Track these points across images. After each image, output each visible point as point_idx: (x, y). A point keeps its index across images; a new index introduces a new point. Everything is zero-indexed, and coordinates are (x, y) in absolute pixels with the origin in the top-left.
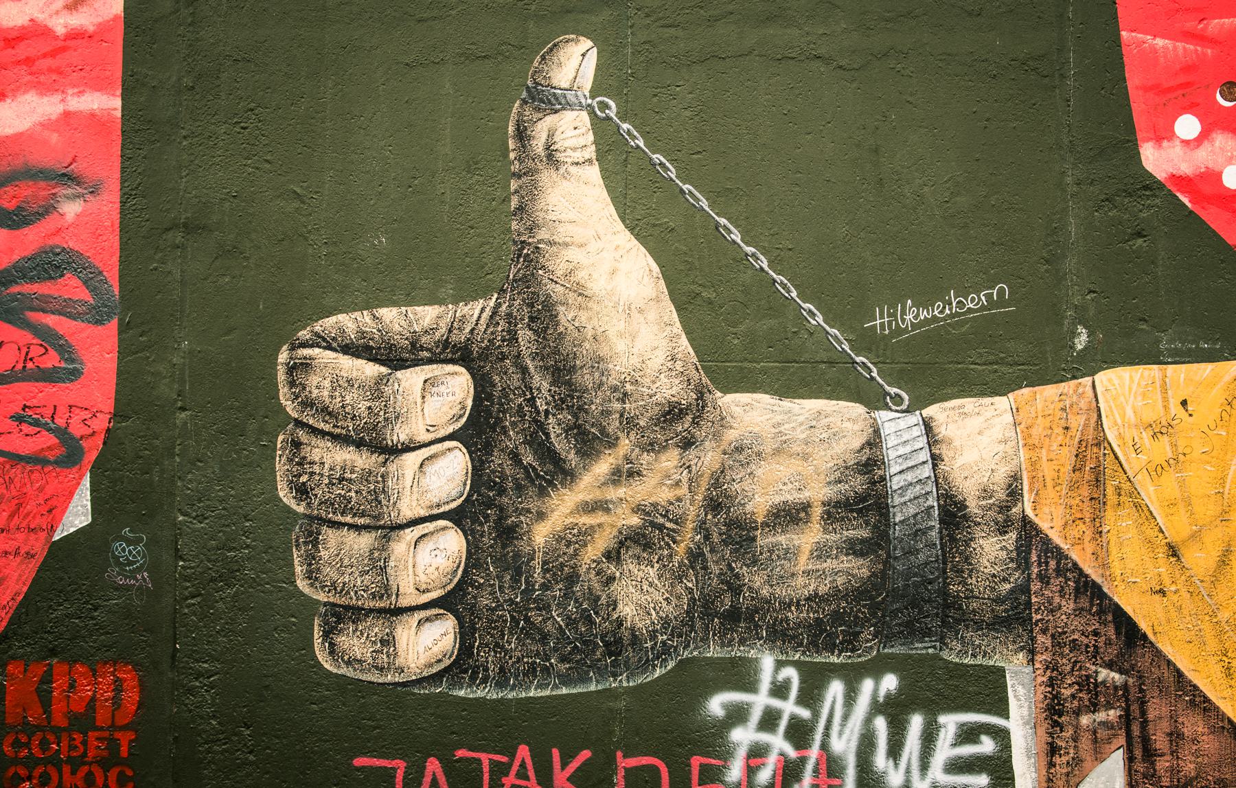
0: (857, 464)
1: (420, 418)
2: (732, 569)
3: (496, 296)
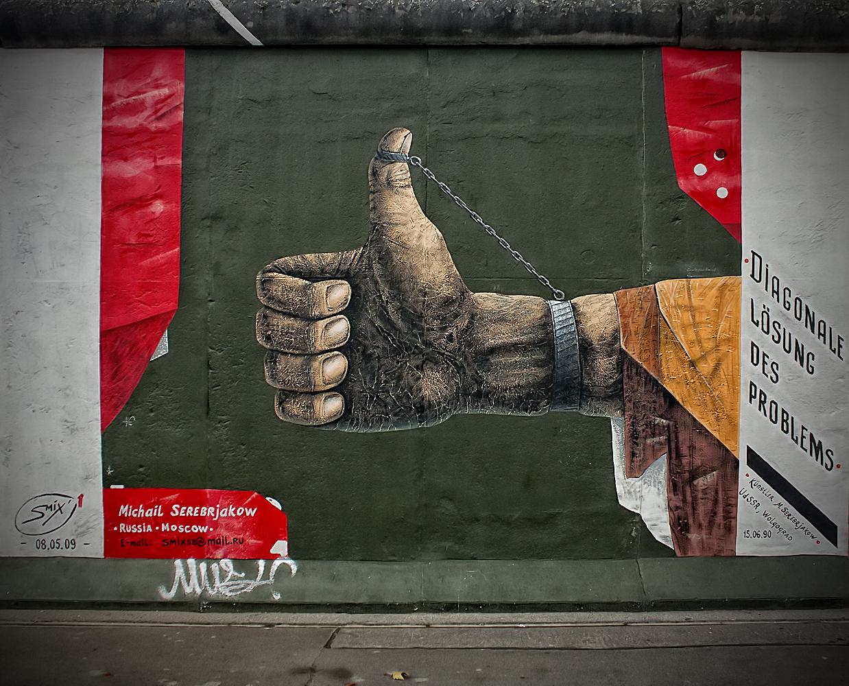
1: (325, 305)
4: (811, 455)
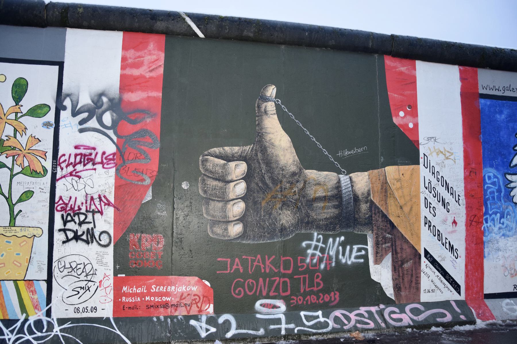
0: (335, 187)
2: (307, 212)
3: (253, 145)
4: (449, 251)
